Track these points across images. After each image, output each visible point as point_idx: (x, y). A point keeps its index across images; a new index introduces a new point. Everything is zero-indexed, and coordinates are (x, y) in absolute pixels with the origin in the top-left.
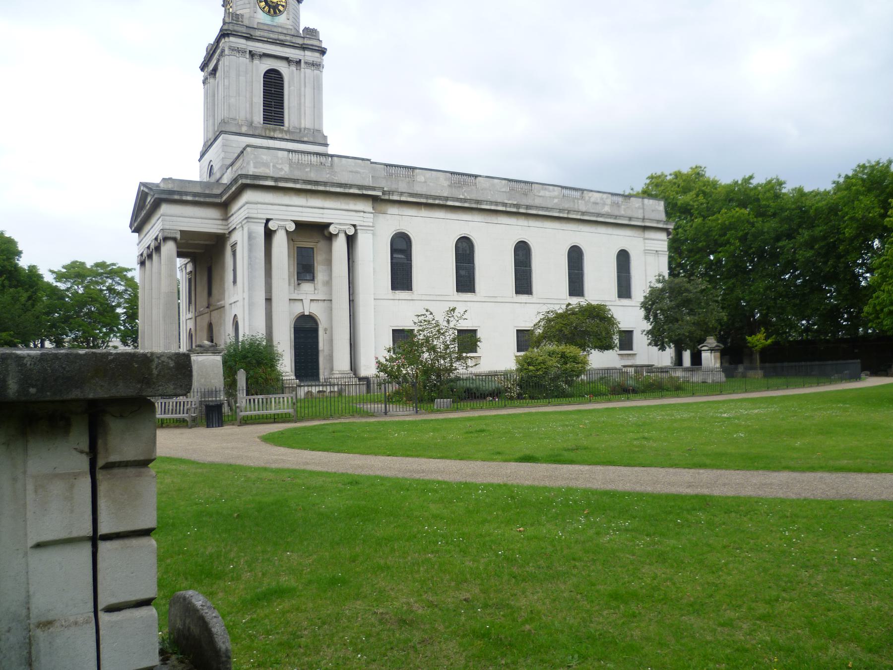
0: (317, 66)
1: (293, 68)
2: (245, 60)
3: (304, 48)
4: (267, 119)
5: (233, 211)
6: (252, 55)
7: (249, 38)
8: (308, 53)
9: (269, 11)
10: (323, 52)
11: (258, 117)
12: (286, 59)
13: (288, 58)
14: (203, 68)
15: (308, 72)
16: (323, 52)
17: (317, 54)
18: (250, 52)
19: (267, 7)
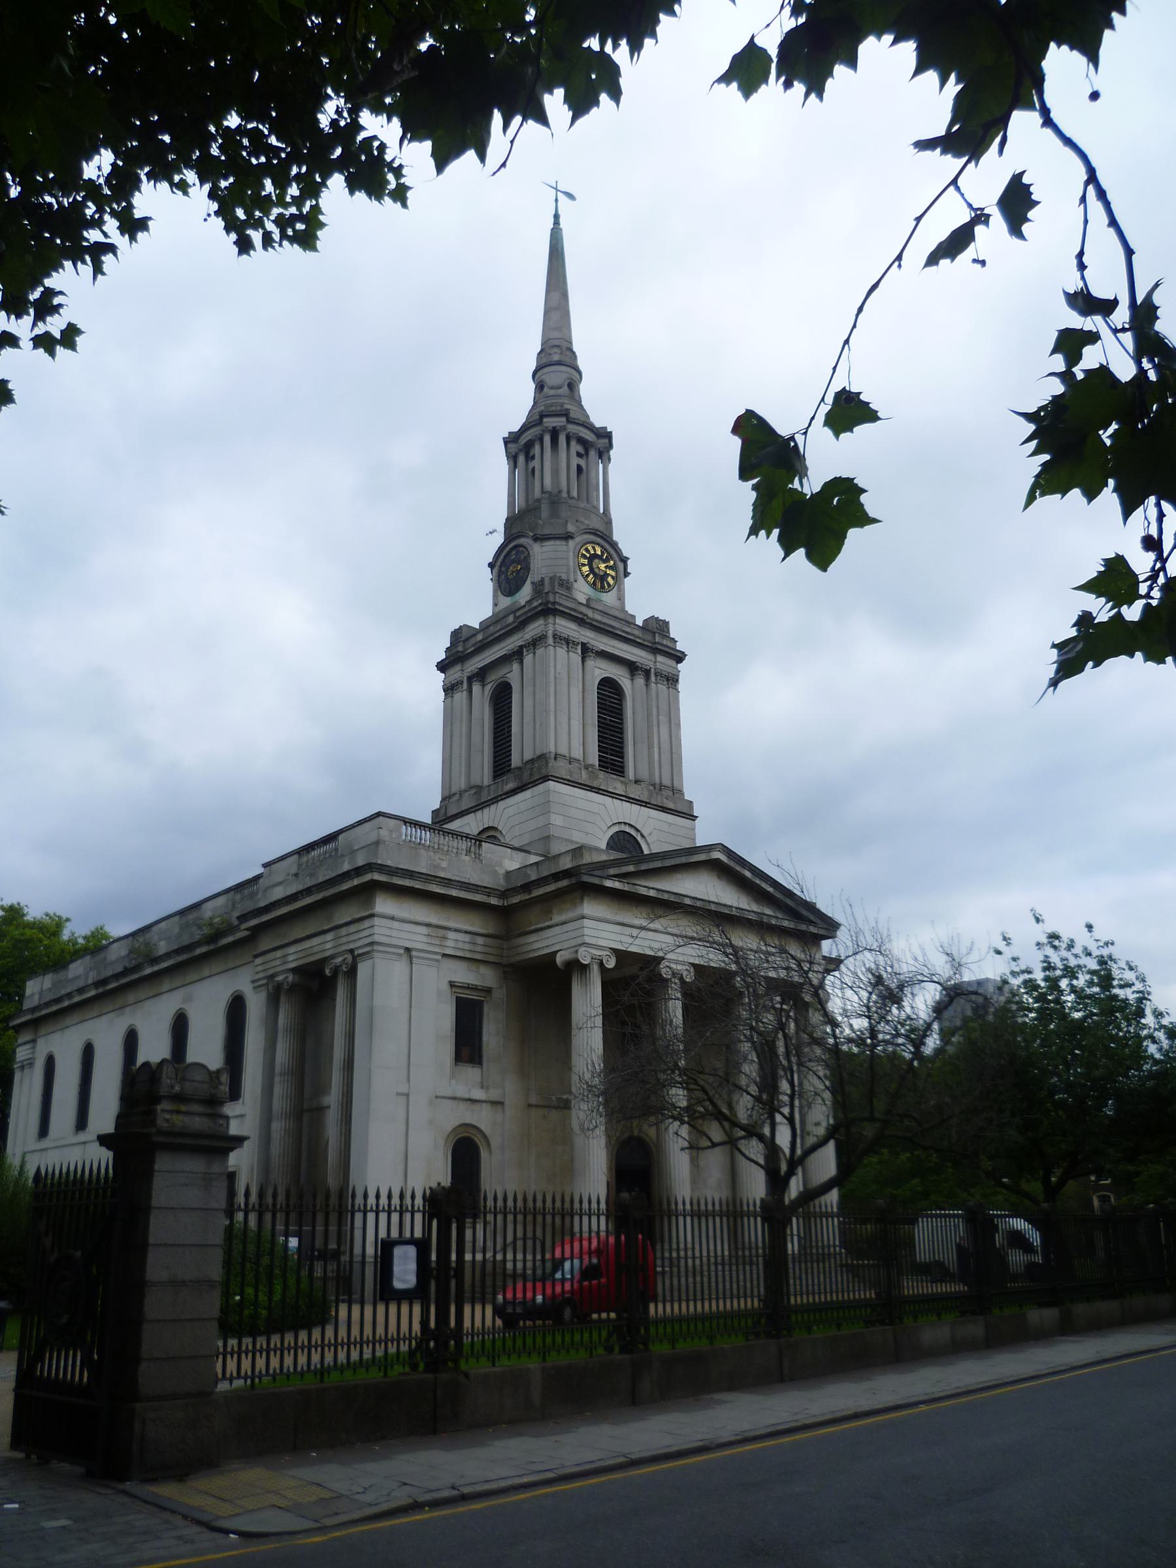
0: (672, 680)
1: (640, 681)
2: (576, 658)
3: (655, 650)
4: (605, 764)
5: (557, 919)
6: (586, 650)
7: (581, 621)
8: (660, 658)
9: (594, 583)
10: (679, 658)
11: (594, 758)
12: (632, 668)
13: (634, 663)
14: (442, 667)
15: (662, 688)
16: (679, 658)
17: (672, 663)
18: (584, 645)
19: (591, 576)
